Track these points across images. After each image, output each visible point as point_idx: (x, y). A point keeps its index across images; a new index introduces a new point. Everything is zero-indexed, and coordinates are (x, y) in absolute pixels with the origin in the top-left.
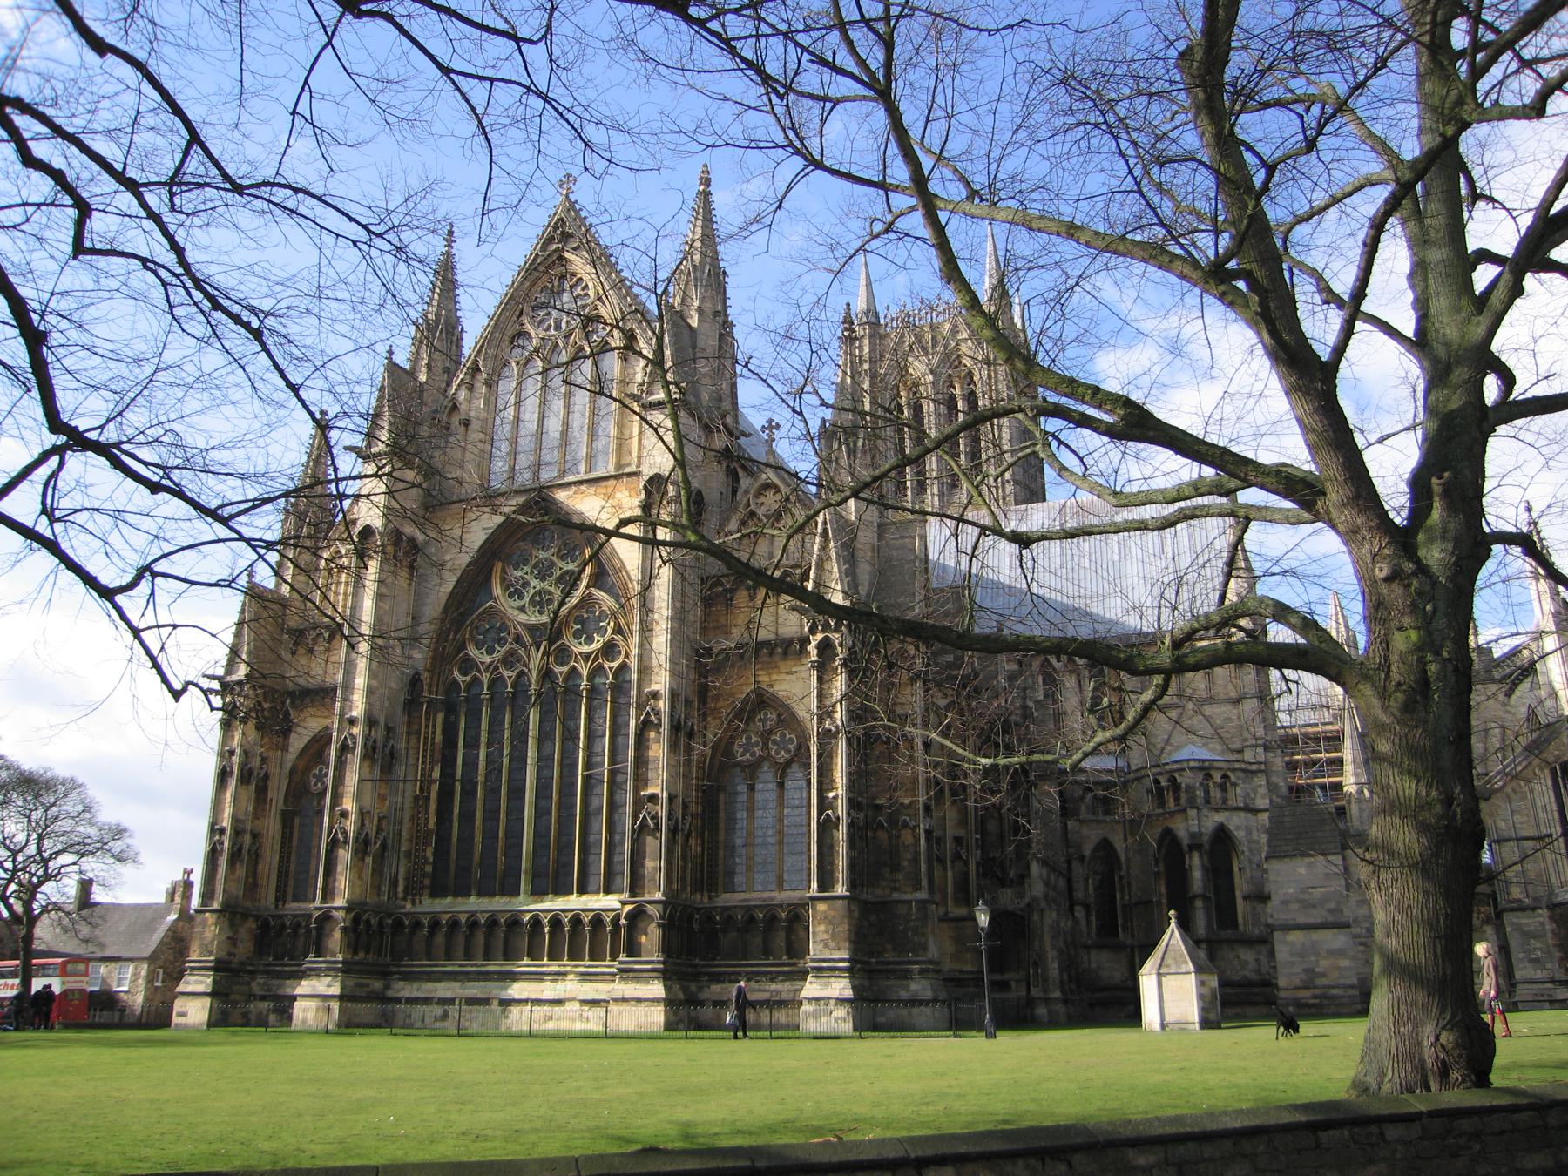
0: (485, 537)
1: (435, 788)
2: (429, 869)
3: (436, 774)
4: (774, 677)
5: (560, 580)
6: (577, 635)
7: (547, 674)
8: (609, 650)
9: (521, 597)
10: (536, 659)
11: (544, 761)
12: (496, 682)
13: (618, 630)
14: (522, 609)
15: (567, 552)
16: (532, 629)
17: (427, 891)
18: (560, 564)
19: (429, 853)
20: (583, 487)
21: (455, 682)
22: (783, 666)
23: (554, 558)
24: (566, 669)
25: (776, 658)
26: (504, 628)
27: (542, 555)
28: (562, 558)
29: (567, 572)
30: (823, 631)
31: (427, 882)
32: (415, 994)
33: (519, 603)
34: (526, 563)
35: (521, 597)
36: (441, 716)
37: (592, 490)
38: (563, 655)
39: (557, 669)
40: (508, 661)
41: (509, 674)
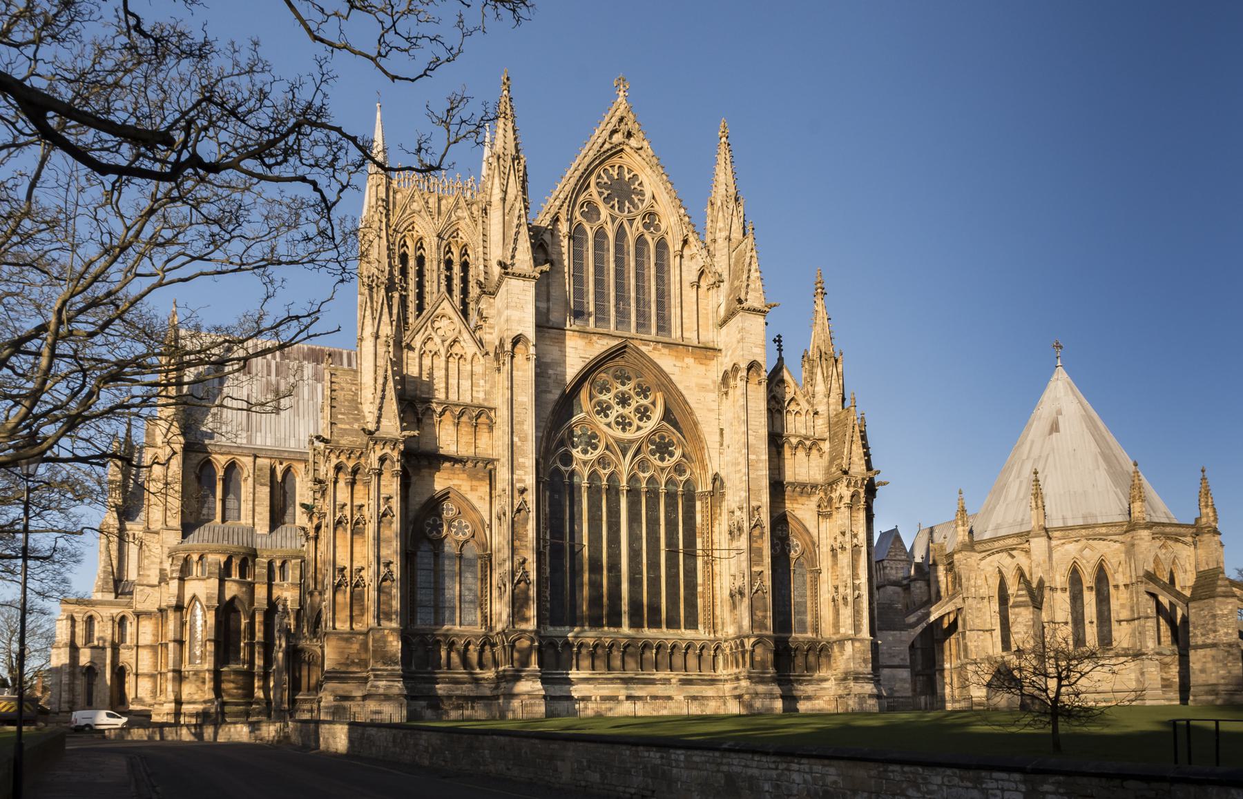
0: (583, 364)
1: (548, 548)
2: (548, 605)
3: (548, 537)
4: (795, 506)
5: (637, 410)
6: (653, 453)
7: (633, 478)
8: (679, 469)
9: (607, 416)
10: (625, 467)
11: (634, 538)
12: (593, 476)
13: (684, 455)
14: (609, 425)
15: (643, 392)
16: (618, 441)
17: (548, 621)
18: (637, 398)
19: (548, 594)
20: (660, 346)
21: (557, 469)
22: (801, 500)
23: (632, 392)
24: (647, 475)
25: (796, 494)
26: (595, 436)
27: (621, 388)
28: (638, 394)
29: (641, 406)
30: (854, 486)
31: (548, 615)
32: (559, 694)
33: (634, 427)
34: (608, 390)
35: (607, 416)
36: (548, 493)
37: (665, 351)
38: (643, 465)
39: (641, 475)
40: (602, 461)
41: (604, 473)
